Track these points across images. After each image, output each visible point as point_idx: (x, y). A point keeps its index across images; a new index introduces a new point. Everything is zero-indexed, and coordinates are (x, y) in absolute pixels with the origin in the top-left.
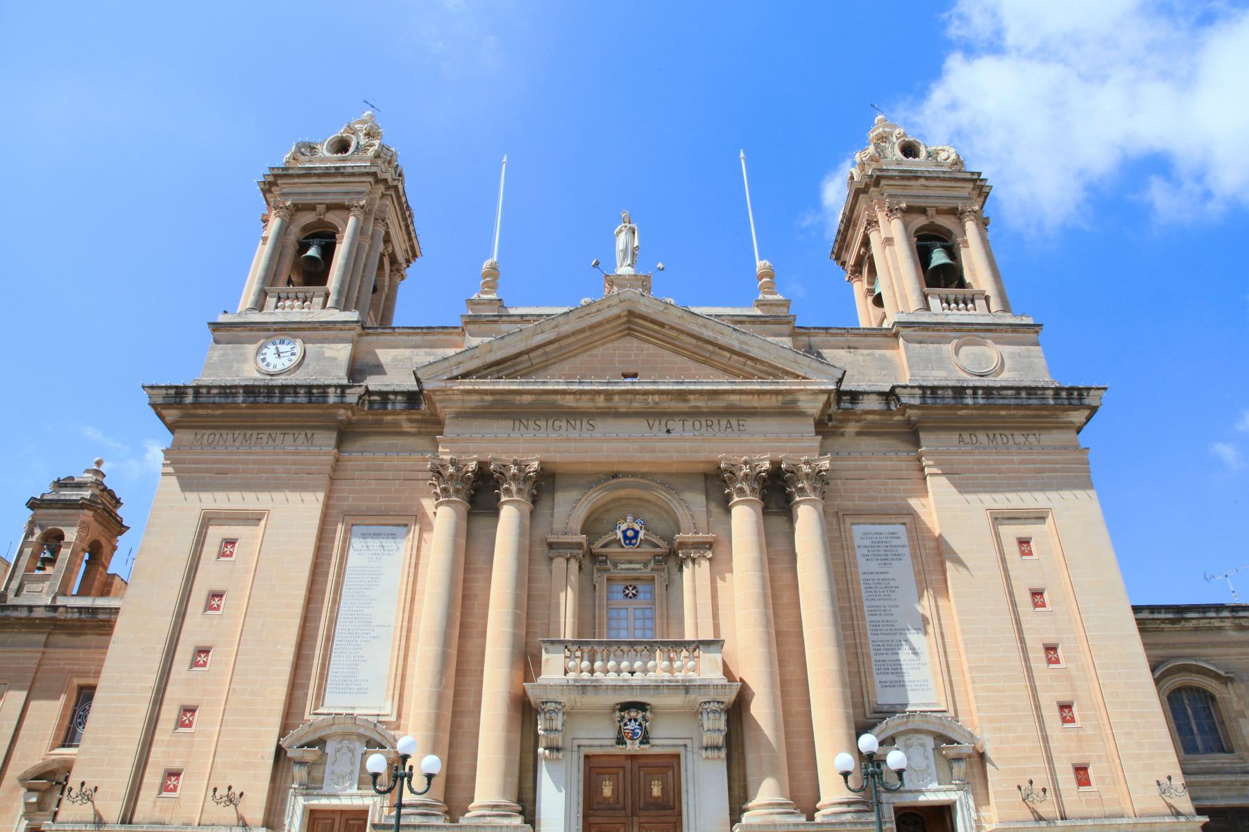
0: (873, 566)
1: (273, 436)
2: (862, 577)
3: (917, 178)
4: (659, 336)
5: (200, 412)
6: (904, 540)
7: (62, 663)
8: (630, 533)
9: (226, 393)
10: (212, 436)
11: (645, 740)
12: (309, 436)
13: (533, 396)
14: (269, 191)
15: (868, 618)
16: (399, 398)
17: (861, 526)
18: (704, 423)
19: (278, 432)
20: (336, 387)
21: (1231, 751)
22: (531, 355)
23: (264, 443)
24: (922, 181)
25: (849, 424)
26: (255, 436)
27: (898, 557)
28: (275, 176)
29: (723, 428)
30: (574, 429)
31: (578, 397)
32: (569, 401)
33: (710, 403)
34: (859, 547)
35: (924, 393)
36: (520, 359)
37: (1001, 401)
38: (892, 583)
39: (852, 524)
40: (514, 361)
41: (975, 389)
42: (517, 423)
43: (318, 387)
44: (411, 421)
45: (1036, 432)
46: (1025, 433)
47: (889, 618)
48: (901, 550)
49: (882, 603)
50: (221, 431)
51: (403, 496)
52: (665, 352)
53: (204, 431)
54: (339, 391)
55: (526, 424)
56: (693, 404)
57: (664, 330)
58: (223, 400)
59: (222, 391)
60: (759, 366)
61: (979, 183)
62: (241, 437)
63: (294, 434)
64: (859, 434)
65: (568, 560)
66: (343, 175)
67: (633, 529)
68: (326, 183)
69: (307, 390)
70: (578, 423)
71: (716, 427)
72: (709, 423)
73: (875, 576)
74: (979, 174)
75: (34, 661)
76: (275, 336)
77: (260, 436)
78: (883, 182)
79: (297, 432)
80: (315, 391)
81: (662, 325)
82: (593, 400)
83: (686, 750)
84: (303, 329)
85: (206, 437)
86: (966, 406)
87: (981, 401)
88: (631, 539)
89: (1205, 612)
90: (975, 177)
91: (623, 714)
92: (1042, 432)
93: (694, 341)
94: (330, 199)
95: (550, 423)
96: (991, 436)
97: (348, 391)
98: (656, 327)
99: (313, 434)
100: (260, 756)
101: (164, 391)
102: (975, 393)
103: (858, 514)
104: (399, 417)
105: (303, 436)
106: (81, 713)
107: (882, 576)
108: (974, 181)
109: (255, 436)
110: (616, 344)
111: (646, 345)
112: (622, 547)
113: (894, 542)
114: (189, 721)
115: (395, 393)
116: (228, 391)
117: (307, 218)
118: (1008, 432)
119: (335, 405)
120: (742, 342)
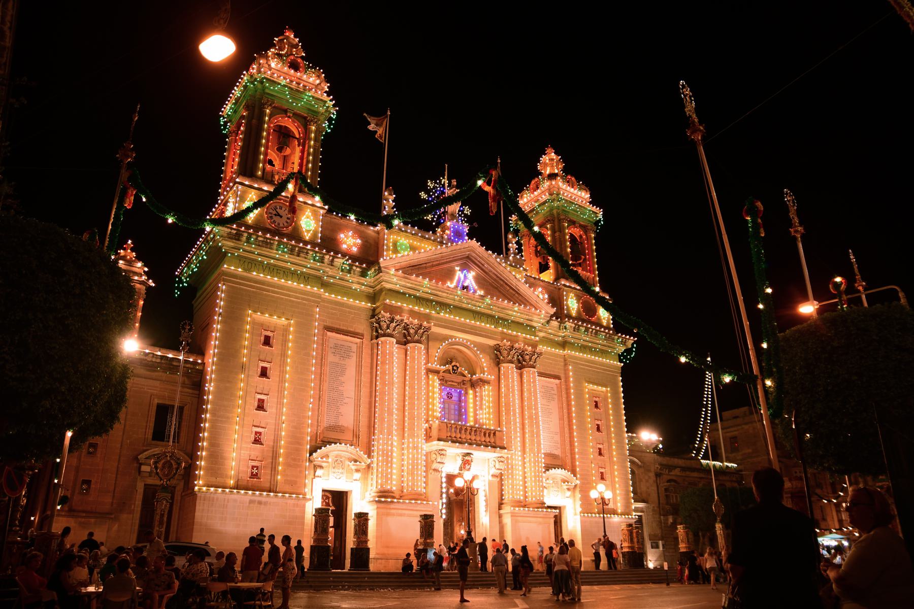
6: (555, 392)
8: (455, 368)
9: (266, 242)
10: (250, 264)
107: (549, 407)
113: (553, 392)
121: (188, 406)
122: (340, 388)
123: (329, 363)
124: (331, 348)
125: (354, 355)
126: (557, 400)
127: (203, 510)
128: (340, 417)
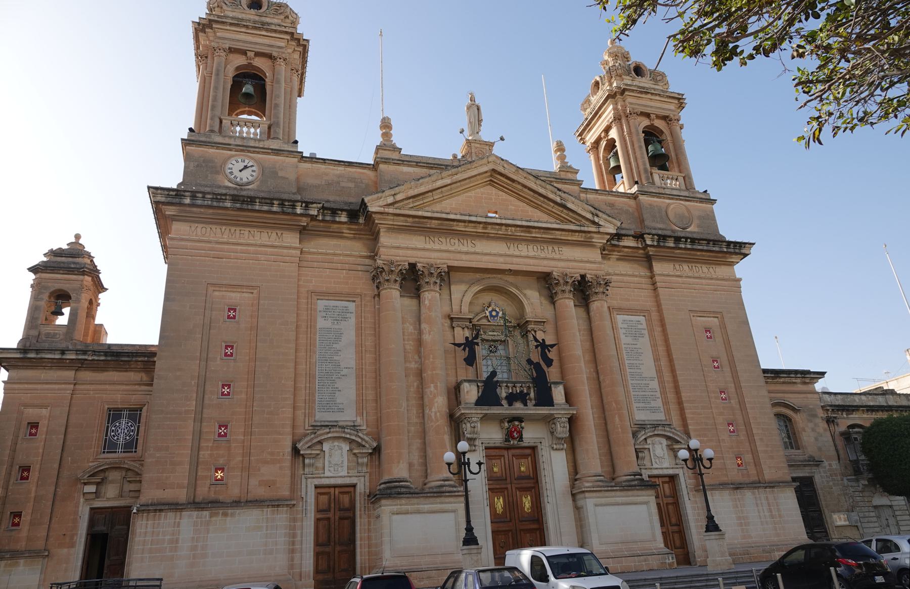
0: (629, 340)
1: (253, 233)
2: (624, 346)
3: (647, 93)
4: (510, 188)
5: (195, 209)
6: (644, 326)
7: (92, 392)
8: (494, 313)
9: (217, 199)
10: (204, 229)
11: (521, 438)
12: (279, 235)
13: (439, 222)
14: (203, 31)
15: (628, 370)
16: (344, 213)
17: (622, 316)
18: (539, 247)
19: (255, 230)
20: (302, 202)
21: (799, 449)
22: (434, 193)
23: (246, 237)
24: (649, 96)
25: (614, 253)
26: (238, 232)
27: (642, 336)
28: (210, 21)
29: (550, 252)
30: (463, 245)
31: (466, 224)
32: (461, 227)
34: (621, 328)
35: (659, 239)
36: (427, 195)
37: (700, 247)
38: (640, 351)
39: (617, 314)
40: (423, 196)
41: (686, 238)
42: (427, 238)
43: (289, 201)
44: (350, 229)
45: (714, 267)
46: (708, 266)
47: (638, 371)
48: (643, 332)
49: (635, 362)
50: (210, 226)
51: (350, 281)
52: (513, 198)
53: (196, 225)
54: (304, 205)
55: (433, 240)
57: (514, 185)
59: (215, 197)
60: (571, 214)
61: (681, 101)
62: (227, 231)
63: (268, 232)
64: (618, 259)
65: (463, 328)
66: (267, 30)
67: (496, 311)
68: (253, 34)
69: (281, 202)
70: (465, 242)
71: (546, 250)
72: (542, 248)
73: (630, 346)
74: (683, 95)
75: (68, 392)
76: (236, 155)
77: (242, 232)
78: (627, 93)
79: (270, 231)
80: (287, 203)
81: (513, 181)
83: (541, 445)
84: (258, 153)
85: (199, 229)
86: (681, 249)
87: (689, 246)
88: (494, 317)
89: (789, 374)
90: (680, 97)
91: (510, 424)
92: (717, 266)
93: (532, 193)
94: (259, 49)
95: (448, 240)
96: (690, 267)
97: (311, 206)
98: (509, 182)
99: (282, 234)
100: (281, 454)
101: (166, 193)
102: (686, 241)
103: (621, 310)
104: (343, 226)
105: (274, 234)
106: (113, 428)
107: (636, 346)
108: (679, 99)
109: (238, 232)
110: (482, 190)
111: (501, 193)
112: (489, 321)
113: (640, 326)
114: (224, 432)
115: (342, 210)
116: (219, 197)
117: (240, 60)
118: (699, 265)
119: (301, 215)
121: (146, 406)
122: (336, 358)
123: (318, 330)
124: (320, 311)
125: (353, 316)
126: (647, 336)
127: (146, 533)
128: (337, 392)
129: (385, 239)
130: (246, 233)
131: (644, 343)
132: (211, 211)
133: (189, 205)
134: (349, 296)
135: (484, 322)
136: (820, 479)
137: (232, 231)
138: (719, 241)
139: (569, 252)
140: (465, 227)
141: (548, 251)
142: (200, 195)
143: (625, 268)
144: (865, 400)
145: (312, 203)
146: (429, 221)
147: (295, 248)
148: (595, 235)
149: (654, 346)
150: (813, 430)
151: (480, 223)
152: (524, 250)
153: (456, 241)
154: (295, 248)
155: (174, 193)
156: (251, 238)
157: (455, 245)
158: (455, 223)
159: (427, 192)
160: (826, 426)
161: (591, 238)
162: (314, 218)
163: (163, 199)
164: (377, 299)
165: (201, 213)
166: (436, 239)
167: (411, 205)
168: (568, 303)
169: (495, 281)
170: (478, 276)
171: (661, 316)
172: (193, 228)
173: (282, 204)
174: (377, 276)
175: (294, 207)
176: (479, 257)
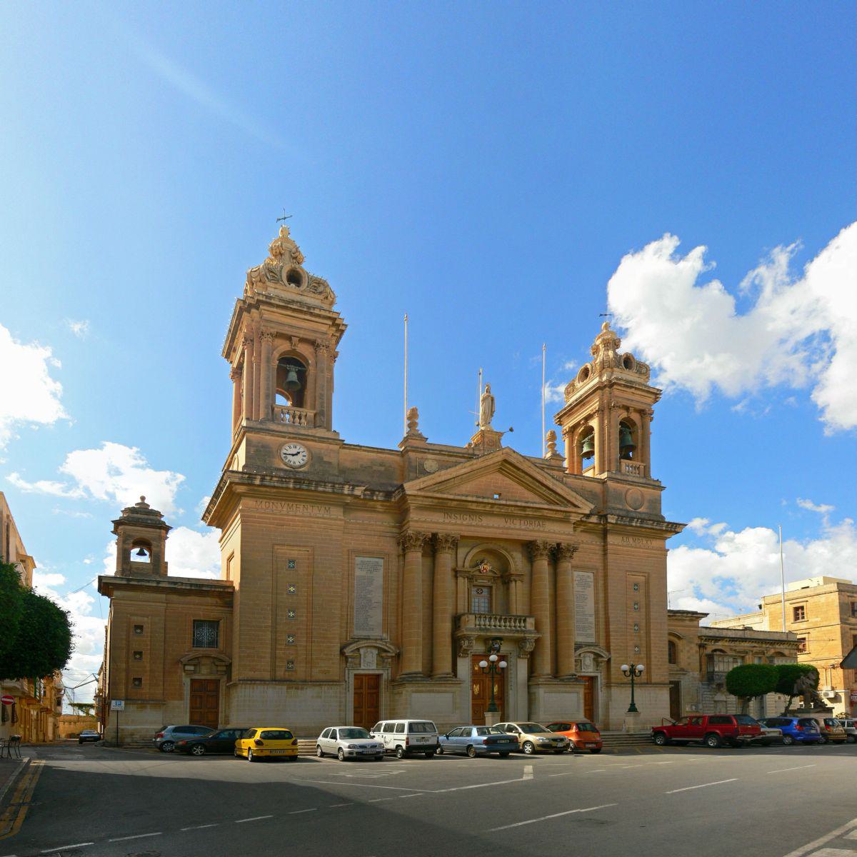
6: (592, 580)
32: (474, 507)
33: (535, 514)
42: (446, 515)
48: (591, 584)
56: (527, 513)
58: (280, 485)
60: (557, 497)
62: (286, 505)
70: (475, 518)
82: (485, 507)
85: (263, 503)
95: (462, 516)
97: (357, 488)
101: (240, 475)
109: (294, 505)
113: (589, 580)
119: (348, 495)
120: (554, 484)
129: (413, 515)
130: (302, 507)
131: (590, 592)
132: (275, 490)
133: (259, 486)
134: (380, 555)
135: (477, 573)
136: (685, 683)
137: (290, 505)
138: (660, 520)
139: (550, 526)
140: (477, 506)
141: (534, 526)
142: (268, 478)
143: (586, 538)
144: (730, 634)
145: (358, 486)
146: (450, 502)
147: (341, 520)
148: (573, 515)
149: (596, 594)
150: (688, 652)
151: (489, 503)
152: (517, 524)
153: (468, 517)
154: (341, 520)
155: (247, 476)
156: (305, 511)
157: (467, 520)
158: (470, 504)
159: (451, 479)
160: (698, 649)
161: (570, 516)
162: (357, 497)
163: (237, 480)
164: (401, 558)
165: (266, 492)
166: (453, 515)
167: (436, 489)
168: (543, 564)
169: (491, 546)
170: (478, 542)
171: (605, 573)
172: (259, 503)
173: (333, 487)
174: (404, 543)
175: (342, 488)
176: (483, 529)
